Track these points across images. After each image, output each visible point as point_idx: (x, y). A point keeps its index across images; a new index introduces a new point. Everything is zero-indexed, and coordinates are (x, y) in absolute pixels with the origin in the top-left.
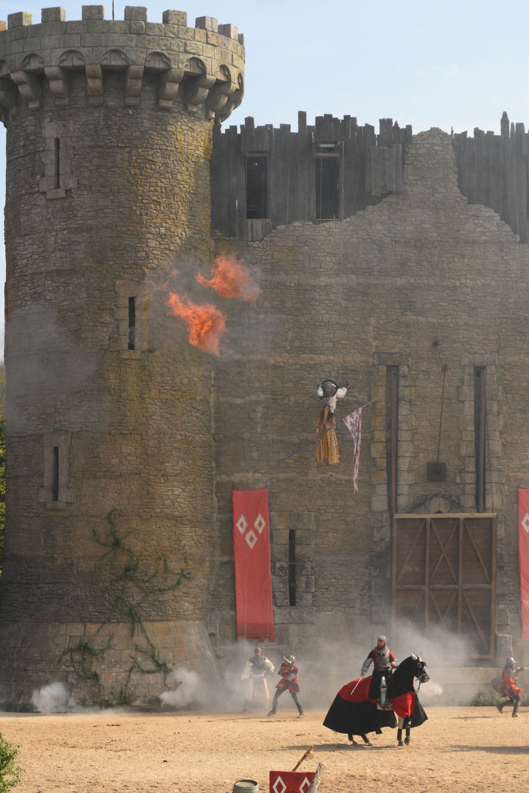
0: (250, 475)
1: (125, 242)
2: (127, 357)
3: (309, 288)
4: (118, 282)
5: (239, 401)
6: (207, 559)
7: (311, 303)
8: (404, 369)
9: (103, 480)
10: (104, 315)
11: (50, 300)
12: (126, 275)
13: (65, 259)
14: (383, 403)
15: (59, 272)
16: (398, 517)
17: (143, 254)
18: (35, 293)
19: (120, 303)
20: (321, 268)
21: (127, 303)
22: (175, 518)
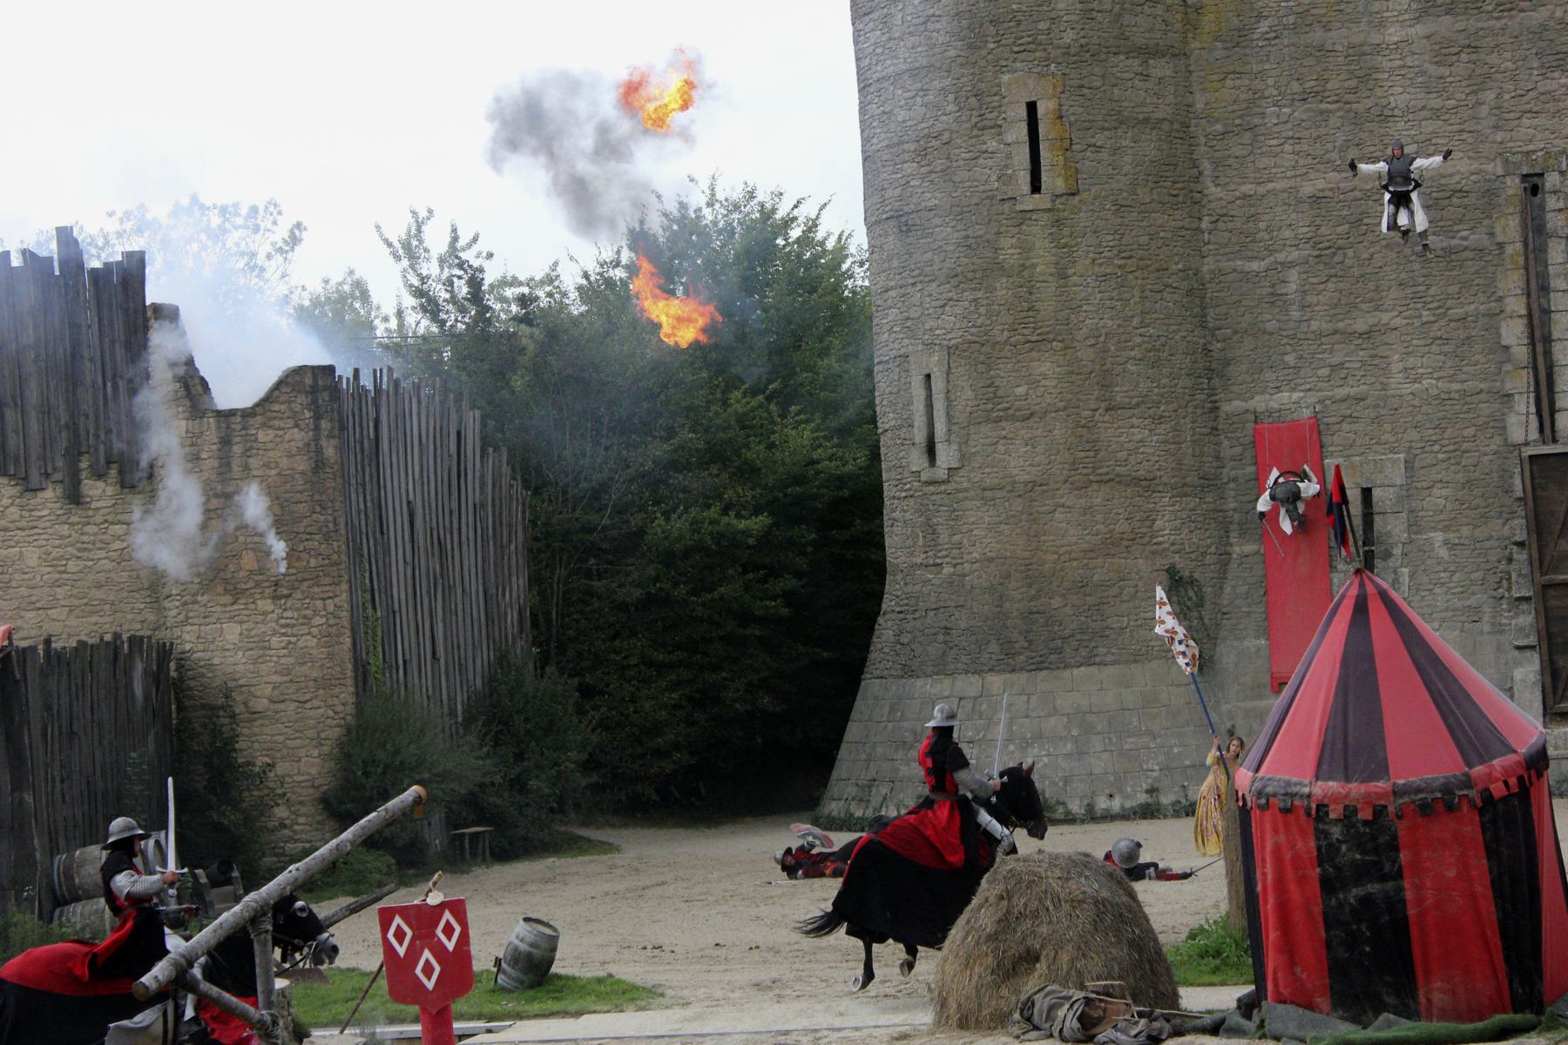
0: (1284, 396)
1: (1014, 7)
2: (1030, 208)
3: (1367, 49)
4: (1006, 78)
5: (1255, 266)
6: (1213, 549)
7: (1375, 76)
8: (1552, 180)
9: (1003, 424)
10: (985, 138)
11: (904, 122)
12: (1018, 65)
13: (919, 49)
14: (1519, 246)
15: (914, 72)
16: (1530, 453)
17: (1043, 26)
18: (884, 113)
19: (1010, 114)
20: (1387, 10)
21: (1023, 113)
22: (1137, 481)
